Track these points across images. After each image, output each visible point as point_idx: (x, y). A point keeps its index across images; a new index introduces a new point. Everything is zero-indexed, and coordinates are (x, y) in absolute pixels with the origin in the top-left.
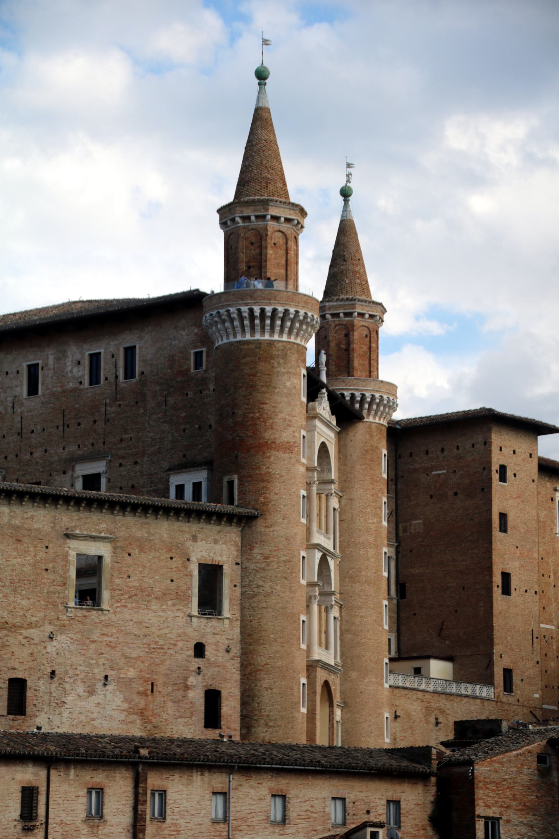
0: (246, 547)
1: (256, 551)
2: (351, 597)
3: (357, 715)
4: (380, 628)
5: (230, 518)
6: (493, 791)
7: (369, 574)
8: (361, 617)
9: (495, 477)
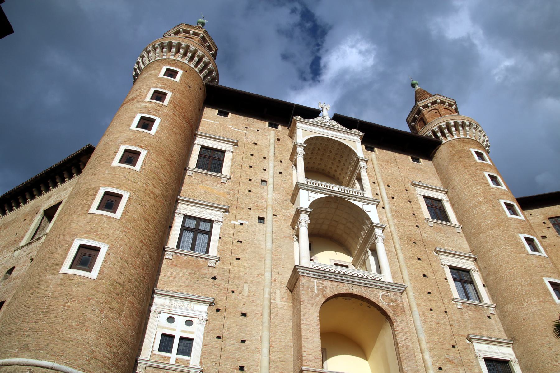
2: (480, 247)
3: (529, 344)
4: (523, 255)
7: (489, 222)
8: (495, 256)
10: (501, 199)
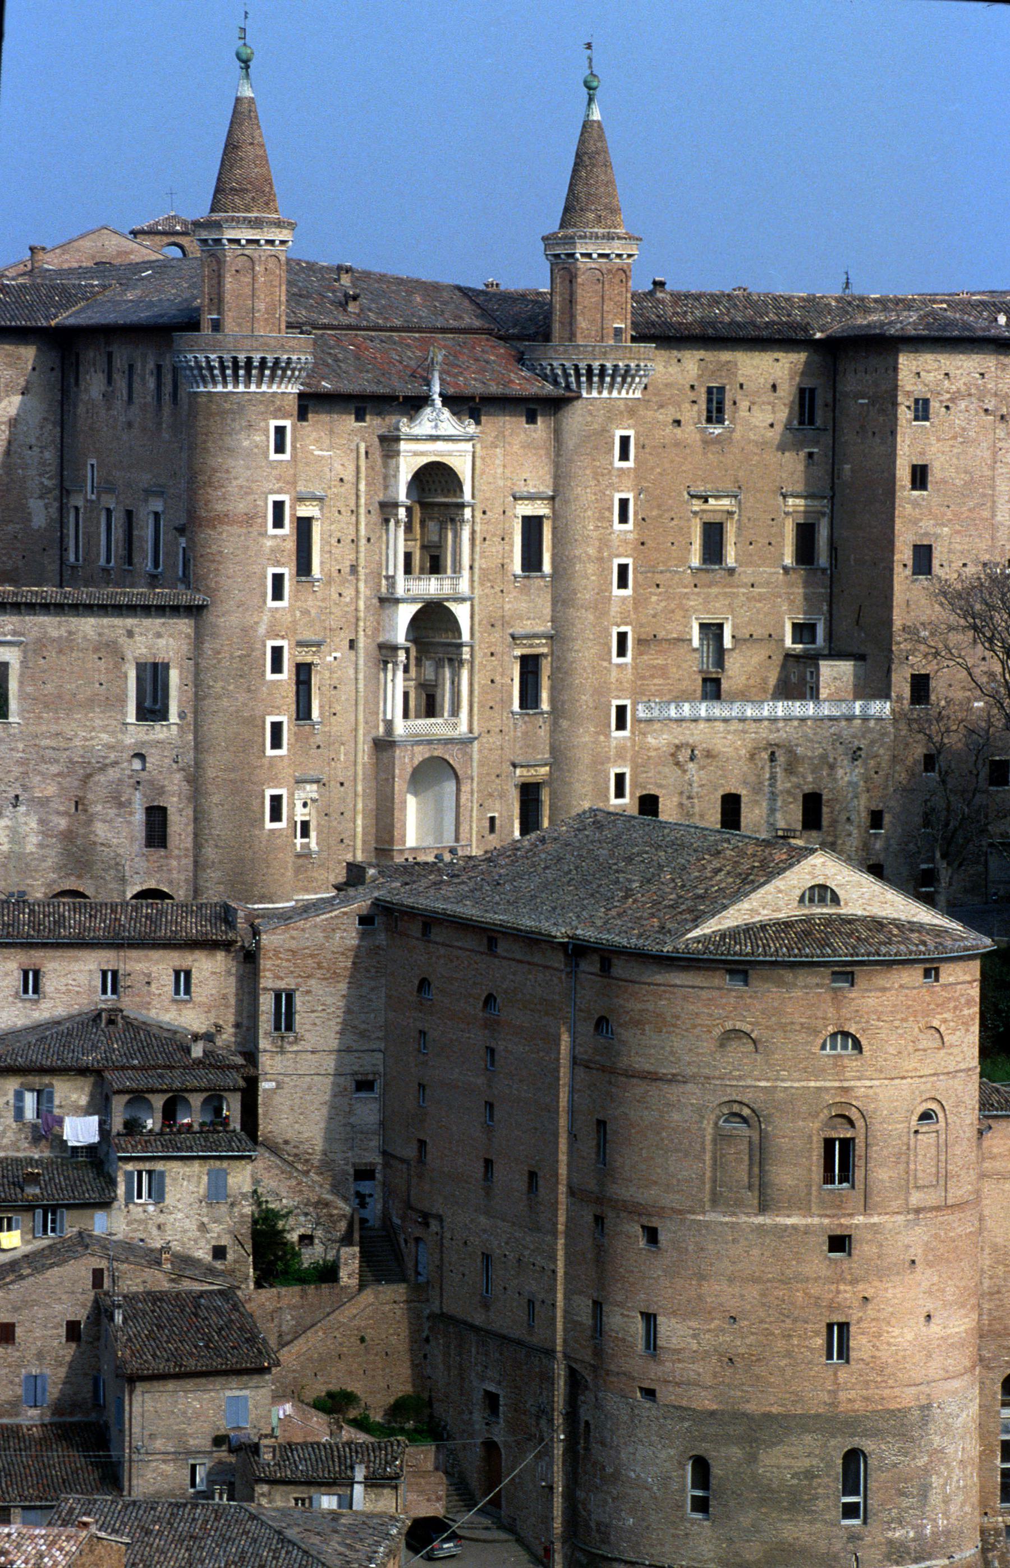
0: (198, 640)
1: (207, 645)
4: (605, 664)
5: (175, 610)
6: (288, 960)
9: (904, 414)
10: (618, 556)
